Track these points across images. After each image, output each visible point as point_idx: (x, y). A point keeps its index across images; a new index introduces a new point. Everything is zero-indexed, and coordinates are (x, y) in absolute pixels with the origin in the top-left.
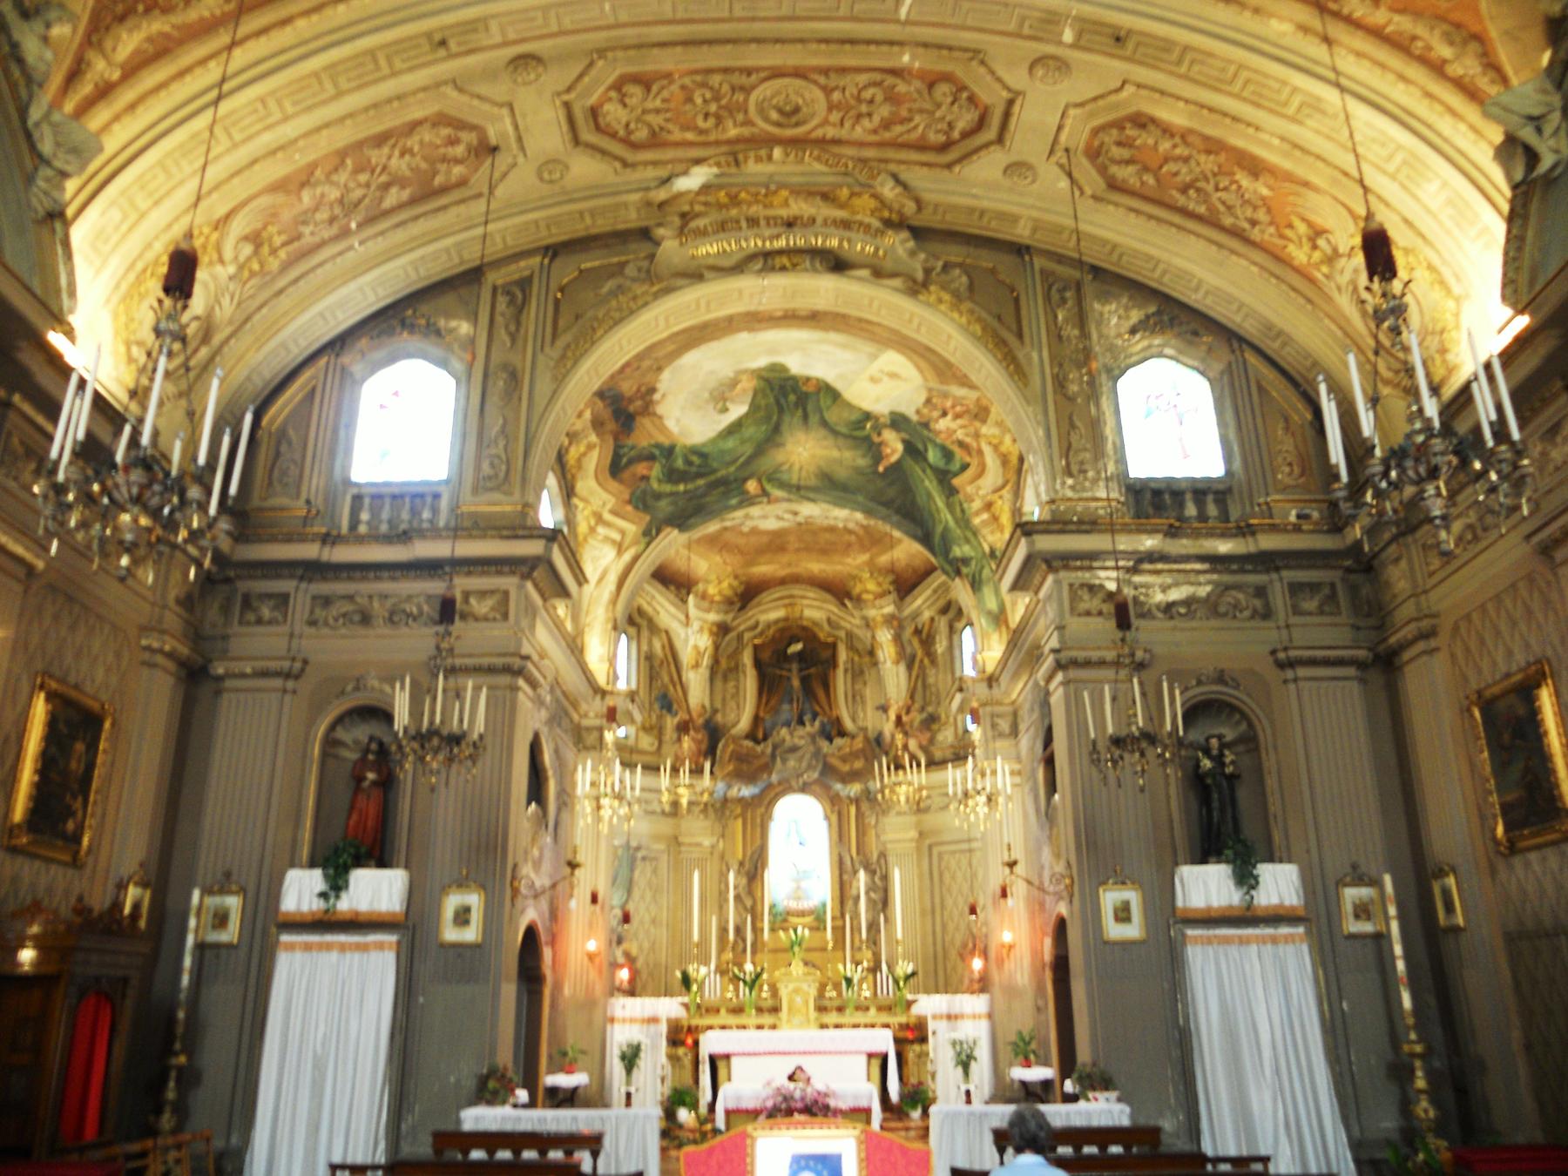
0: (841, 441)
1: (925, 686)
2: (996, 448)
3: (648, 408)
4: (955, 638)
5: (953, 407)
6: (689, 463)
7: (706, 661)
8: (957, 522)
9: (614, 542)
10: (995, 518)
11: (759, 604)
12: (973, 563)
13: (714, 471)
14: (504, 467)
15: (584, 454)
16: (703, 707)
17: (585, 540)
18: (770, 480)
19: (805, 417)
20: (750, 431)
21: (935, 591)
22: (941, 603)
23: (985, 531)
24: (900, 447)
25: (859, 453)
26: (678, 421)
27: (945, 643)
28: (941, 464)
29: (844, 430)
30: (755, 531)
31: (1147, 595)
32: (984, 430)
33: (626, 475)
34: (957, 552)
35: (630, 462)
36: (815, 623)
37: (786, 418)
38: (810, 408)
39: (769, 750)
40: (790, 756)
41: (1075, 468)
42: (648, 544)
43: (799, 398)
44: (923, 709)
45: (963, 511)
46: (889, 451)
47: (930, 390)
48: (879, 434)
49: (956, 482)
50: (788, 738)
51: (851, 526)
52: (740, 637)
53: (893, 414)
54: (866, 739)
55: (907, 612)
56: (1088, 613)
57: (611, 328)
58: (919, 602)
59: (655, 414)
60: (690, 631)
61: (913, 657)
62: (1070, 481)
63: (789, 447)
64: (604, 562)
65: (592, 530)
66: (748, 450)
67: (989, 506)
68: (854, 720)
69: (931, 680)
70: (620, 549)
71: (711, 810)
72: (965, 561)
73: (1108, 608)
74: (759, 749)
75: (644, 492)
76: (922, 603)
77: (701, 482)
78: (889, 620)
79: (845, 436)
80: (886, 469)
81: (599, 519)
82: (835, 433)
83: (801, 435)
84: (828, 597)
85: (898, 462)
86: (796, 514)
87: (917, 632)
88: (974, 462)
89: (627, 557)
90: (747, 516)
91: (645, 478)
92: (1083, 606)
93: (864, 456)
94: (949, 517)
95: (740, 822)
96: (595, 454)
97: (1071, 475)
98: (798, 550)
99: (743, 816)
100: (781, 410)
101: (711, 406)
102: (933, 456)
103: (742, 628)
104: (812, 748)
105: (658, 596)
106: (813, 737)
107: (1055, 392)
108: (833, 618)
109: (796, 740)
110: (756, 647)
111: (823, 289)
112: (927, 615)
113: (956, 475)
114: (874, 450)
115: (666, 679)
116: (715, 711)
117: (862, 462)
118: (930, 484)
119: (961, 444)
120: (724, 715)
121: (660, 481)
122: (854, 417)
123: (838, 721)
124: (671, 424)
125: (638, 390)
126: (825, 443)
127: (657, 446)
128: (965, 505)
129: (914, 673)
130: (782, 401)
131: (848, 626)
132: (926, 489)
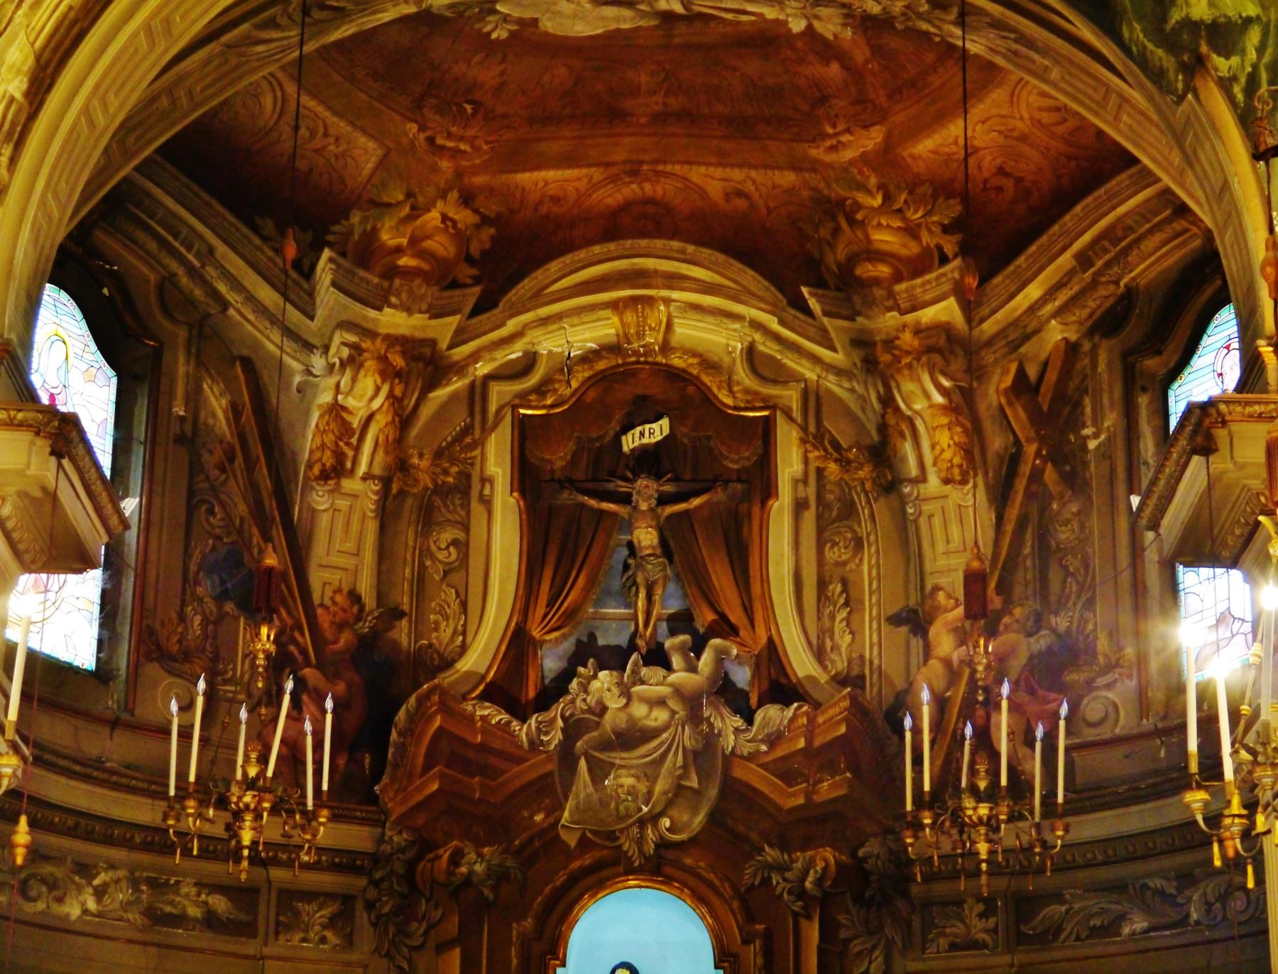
4: (1143, 401)
7: (368, 458)
11: (538, 298)
12: (1253, 37)
16: (354, 597)
21: (1084, 260)
22: (1104, 296)
27: (1111, 419)
36: (709, 364)
39: (554, 738)
40: (618, 757)
50: (614, 703)
52: (477, 394)
54: (858, 709)
55: (989, 327)
58: (1034, 291)
60: (318, 362)
61: (1014, 460)
68: (820, 655)
69: (1064, 535)
71: (362, 918)
74: (523, 731)
76: (1039, 302)
78: (943, 347)
84: (750, 278)
87: (1023, 387)
95: (456, 953)
98: (661, 118)
99: (466, 940)
103: (482, 369)
104: (688, 738)
105: (221, 248)
106: (692, 702)
108: (767, 347)
109: (639, 710)
110: (524, 428)
112: (1055, 334)
115: (242, 508)
116: (397, 614)
129: (1013, 513)
131: (810, 373)
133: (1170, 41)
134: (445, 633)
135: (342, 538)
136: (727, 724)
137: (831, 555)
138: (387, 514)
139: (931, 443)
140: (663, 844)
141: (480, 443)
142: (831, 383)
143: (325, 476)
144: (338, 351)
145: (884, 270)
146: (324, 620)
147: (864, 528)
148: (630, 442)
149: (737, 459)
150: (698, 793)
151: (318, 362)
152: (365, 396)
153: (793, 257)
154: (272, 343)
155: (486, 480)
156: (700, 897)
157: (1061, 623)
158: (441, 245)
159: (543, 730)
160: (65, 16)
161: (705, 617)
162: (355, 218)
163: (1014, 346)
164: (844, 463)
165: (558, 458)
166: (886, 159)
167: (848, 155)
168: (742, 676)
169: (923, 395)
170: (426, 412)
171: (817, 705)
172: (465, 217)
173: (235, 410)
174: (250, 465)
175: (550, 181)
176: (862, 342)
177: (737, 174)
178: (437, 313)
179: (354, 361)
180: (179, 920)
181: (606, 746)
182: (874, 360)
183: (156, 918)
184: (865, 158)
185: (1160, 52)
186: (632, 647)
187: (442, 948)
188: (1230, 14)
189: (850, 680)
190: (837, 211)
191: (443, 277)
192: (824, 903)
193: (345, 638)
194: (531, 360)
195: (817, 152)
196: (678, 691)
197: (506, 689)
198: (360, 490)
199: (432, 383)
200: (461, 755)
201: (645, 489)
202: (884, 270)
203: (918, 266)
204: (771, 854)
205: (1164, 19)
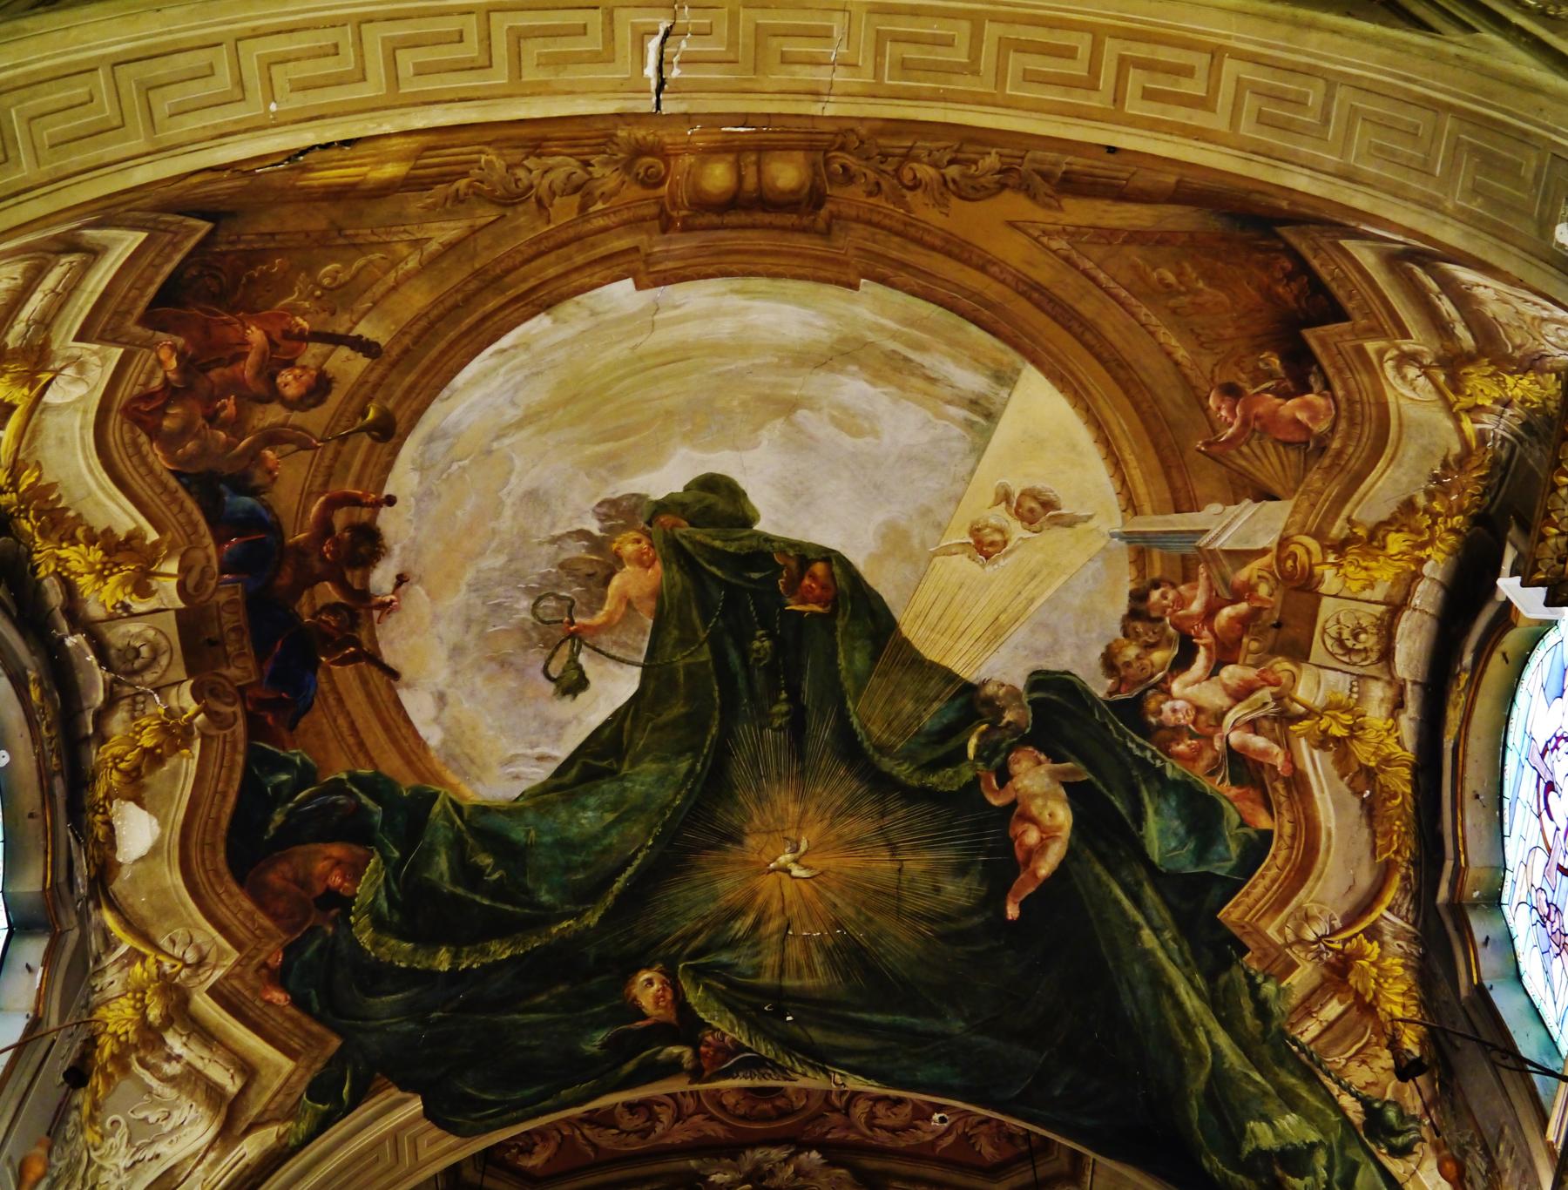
3: (353, 630)
5: (1210, 612)
6: (467, 873)
9: (213, 1093)
10: (1366, 1008)
12: (1321, 1159)
13: (547, 917)
15: (153, 758)
18: (699, 973)
19: (797, 727)
20: (644, 778)
23: (1337, 1059)
24: (1063, 816)
25: (948, 855)
26: (441, 699)
28: (1185, 863)
29: (902, 771)
33: (276, 877)
34: (1262, 1135)
35: (292, 835)
37: (744, 730)
38: (807, 696)
42: (323, 1124)
43: (779, 644)
45: (1263, 1009)
46: (1032, 837)
48: (1004, 776)
49: (1231, 913)
53: (1040, 680)
59: (375, 659)
63: (751, 842)
64: (171, 1152)
65: (150, 1037)
67: (1338, 972)
77: (501, 951)
79: (912, 795)
80: (1023, 906)
81: (179, 1011)
82: (881, 784)
83: (785, 802)
89: (250, 1148)
91: (336, 902)
93: (961, 870)
94: (1223, 1039)
96: (188, 763)
101: (536, 658)
102: (1160, 832)
113: (1231, 887)
114: (989, 834)
117: (956, 891)
119: (1242, 766)
121: (379, 924)
124: (418, 706)
125: (324, 526)
126: (854, 827)
127: (377, 786)
128: (1269, 989)
130: (734, 657)
132: (1147, 954)
160: (241, 1173)
185: (1240, 1177)
188: (1296, 1142)
205: (1237, 1149)
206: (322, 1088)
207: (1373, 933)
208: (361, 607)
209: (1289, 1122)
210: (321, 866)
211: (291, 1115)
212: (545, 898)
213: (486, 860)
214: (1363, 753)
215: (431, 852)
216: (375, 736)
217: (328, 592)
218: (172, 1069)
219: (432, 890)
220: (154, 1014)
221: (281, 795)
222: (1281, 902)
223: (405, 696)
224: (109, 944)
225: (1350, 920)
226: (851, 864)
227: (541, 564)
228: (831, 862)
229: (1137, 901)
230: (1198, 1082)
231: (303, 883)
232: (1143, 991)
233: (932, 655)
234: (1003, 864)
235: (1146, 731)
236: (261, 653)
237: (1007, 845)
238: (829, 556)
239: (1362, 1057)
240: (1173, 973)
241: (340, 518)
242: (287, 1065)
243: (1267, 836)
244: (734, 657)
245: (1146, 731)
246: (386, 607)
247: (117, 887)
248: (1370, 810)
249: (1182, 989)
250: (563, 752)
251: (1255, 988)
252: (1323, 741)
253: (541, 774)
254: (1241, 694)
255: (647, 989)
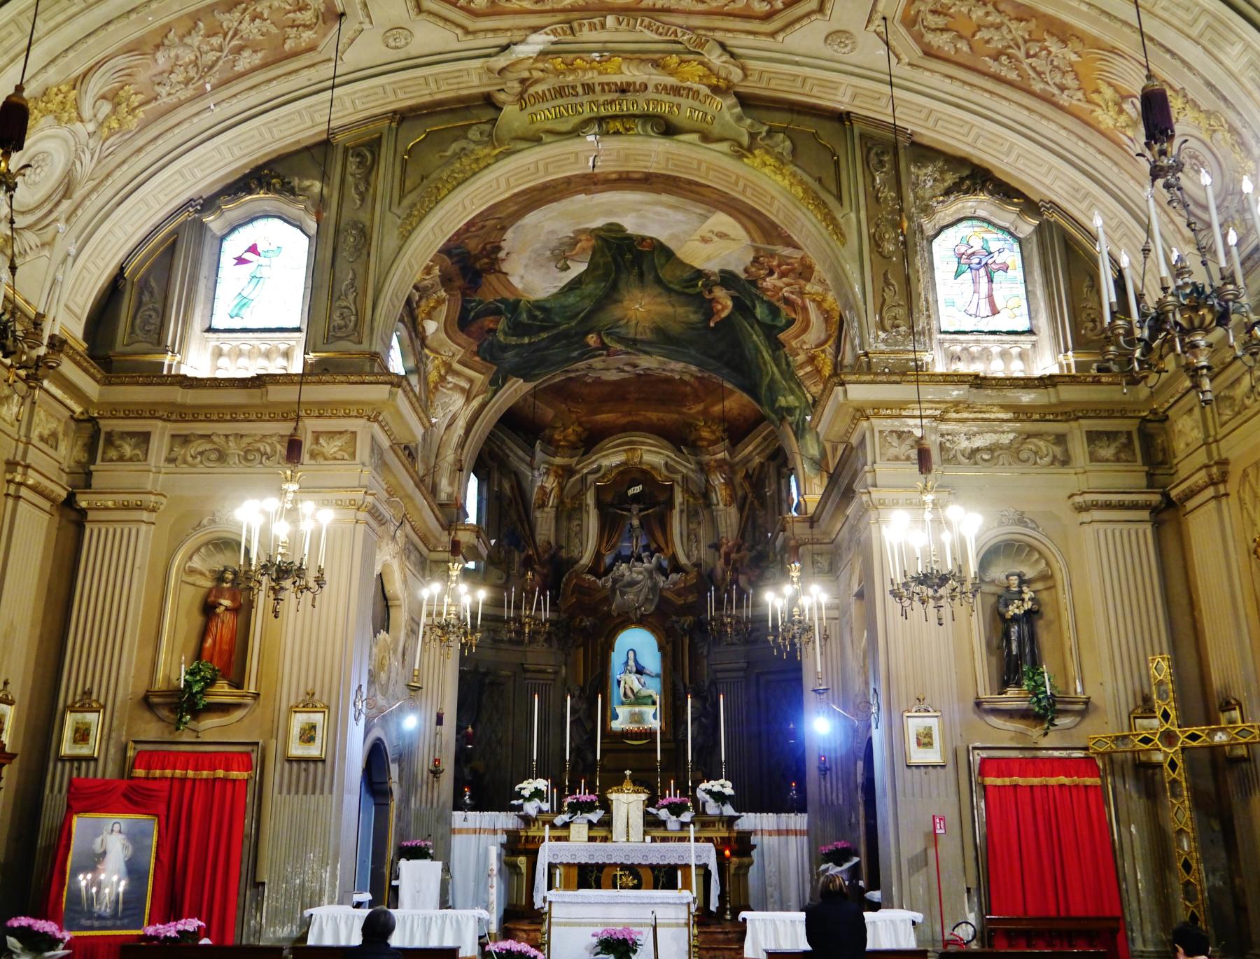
0: (674, 298)
1: (754, 527)
2: (819, 304)
4: (783, 481)
5: (779, 266)
6: (532, 317)
7: (552, 501)
8: (782, 373)
9: (462, 390)
10: (818, 371)
11: (602, 450)
12: (798, 412)
13: (557, 325)
14: (353, 318)
15: (434, 308)
16: (549, 543)
17: (436, 388)
18: (608, 334)
19: (641, 275)
20: (589, 288)
21: (765, 439)
23: (808, 383)
24: (730, 303)
25: (692, 309)
26: (522, 277)
27: (774, 487)
28: (768, 320)
29: (677, 288)
30: (598, 382)
31: (953, 442)
32: (808, 288)
34: (782, 402)
35: (480, 315)
36: (654, 468)
37: (623, 276)
38: (644, 268)
39: (609, 584)
40: (628, 589)
41: (888, 323)
42: (495, 393)
44: (752, 548)
45: (788, 364)
46: (719, 307)
47: (757, 250)
48: (710, 292)
49: (782, 336)
50: (627, 573)
51: (687, 377)
53: (722, 271)
54: (699, 575)
55: (737, 459)
56: (897, 459)
57: (454, 188)
58: (750, 448)
60: (536, 473)
62: (882, 335)
63: (625, 303)
64: (454, 409)
65: (443, 379)
66: (588, 304)
67: (812, 359)
68: (688, 557)
69: (760, 521)
70: (469, 396)
72: (790, 410)
73: (914, 454)
74: (600, 583)
75: (491, 344)
76: (751, 450)
77: (544, 335)
78: (721, 464)
79: (679, 293)
80: (716, 324)
81: (450, 369)
82: (669, 290)
83: (637, 293)
84: (665, 443)
85: (728, 317)
86: (635, 366)
87: (748, 476)
88: (799, 318)
89: (475, 403)
90: (590, 367)
91: (494, 331)
92: (892, 452)
93: (696, 313)
94: (775, 369)
95: (581, 650)
96: (445, 307)
97: (884, 330)
100: (618, 271)
102: (760, 312)
103: (585, 471)
104: (649, 583)
105: (507, 441)
107: (871, 252)
109: (635, 575)
111: (653, 153)
112: (757, 460)
113: (782, 330)
114: (707, 307)
115: (515, 518)
116: (560, 548)
117: (694, 318)
118: (757, 338)
119: (787, 301)
120: (568, 551)
121: (506, 334)
122: (686, 275)
123: (674, 558)
124: (515, 280)
125: (484, 248)
126: (659, 300)
127: (503, 301)
128: (791, 359)
130: (619, 259)
132: (754, 342)
133: (776, 411)
134: (576, 552)
135: (545, 526)
136: (661, 580)
137: (691, 526)
138: (558, 518)
139: (720, 494)
140: (642, 615)
141: (585, 494)
142: (691, 474)
143: (539, 507)
144: (543, 470)
145: (705, 443)
146: (540, 550)
147: (701, 518)
148: (630, 492)
149: (663, 498)
150: (652, 600)
151: (536, 473)
152: (551, 483)
153: (678, 437)
154: (524, 468)
155: (587, 505)
156: (653, 630)
157: (759, 548)
158: (573, 438)
159: (607, 582)
161: (654, 546)
162: (547, 431)
163: (745, 465)
164: (695, 498)
165: (608, 498)
166: (705, 412)
167: (693, 411)
168: (665, 564)
169: (718, 480)
170: (569, 485)
171: (687, 573)
172: (579, 429)
173: (512, 488)
174: (517, 504)
175: (604, 417)
176: (699, 463)
177: (661, 415)
178: (571, 457)
179: (547, 473)
180: (502, 641)
181: (625, 586)
182: (703, 469)
183: (495, 641)
184: (698, 412)
186: (632, 556)
187: (578, 647)
189: (697, 565)
190: (691, 426)
191: (573, 447)
192: (690, 632)
193: (546, 556)
194: (600, 467)
195: (684, 410)
196: (646, 569)
197: (595, 570)
198: (550, 511)
199: (571, 477)
200: (583, 591)
201: (635, 508)
202: (705, 443)
203: (715, 442)
204: (674, 618)
206: (493, 382)
207: (823, 351)
208: (496, 261)
209: (791, 398)
210: (486, 323)
211: (485, 392)
212: (557, 320)
213: (538, 313)
214: (826, 306)
215: (520, 314)
216: (500, 288)
217: (486, 260)
218: (450, 386)
219: (521, 323)
220: (443, 372)
221: (472, 309)
222: (797, 337)
223: (511, 279)
224: (427, 357)
225: (817, 346)
226: (659, 309)
227: (554, 244)
228: (653, 308)
229: (752, 327)
230: (766, 380)
231: (482, 328)
232: (753, 352)
233: (687, 261)
234: (709, 312)
235: (758, 288)
236: (464, 278)
237: (712, 309)
238: (651, 239)
239: (815, 384)
240: (762, 348)
241: (488, 247)
242: (482, 377)
243: (794, 320)
244: (619, 259)
245: (758, 288)
246: (503, 260)
247: (428, 342)
248: (826, 320)
249: (765, 353)
250: (562, 285)
251: (786, 358)
252: (814, 301)
253: (556, 290)
254: (788, 285)
255: (592, 339)
